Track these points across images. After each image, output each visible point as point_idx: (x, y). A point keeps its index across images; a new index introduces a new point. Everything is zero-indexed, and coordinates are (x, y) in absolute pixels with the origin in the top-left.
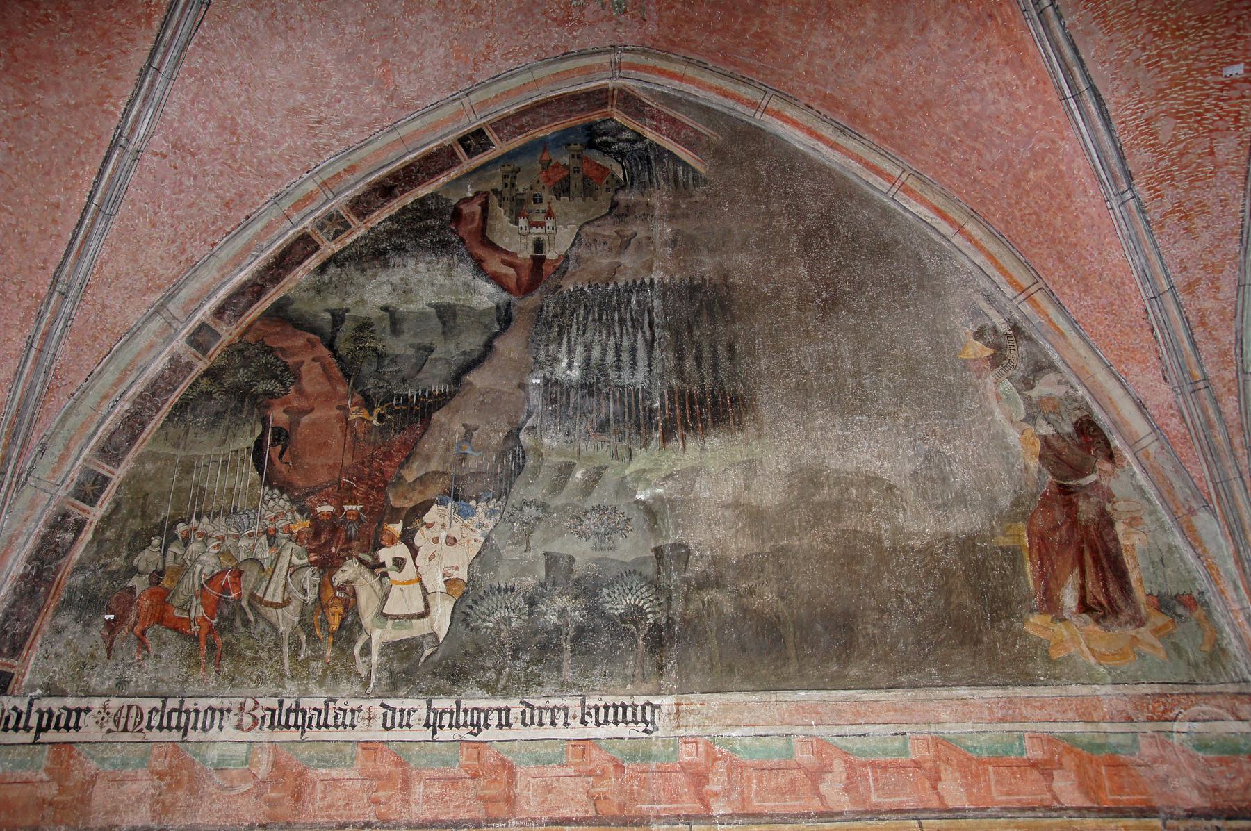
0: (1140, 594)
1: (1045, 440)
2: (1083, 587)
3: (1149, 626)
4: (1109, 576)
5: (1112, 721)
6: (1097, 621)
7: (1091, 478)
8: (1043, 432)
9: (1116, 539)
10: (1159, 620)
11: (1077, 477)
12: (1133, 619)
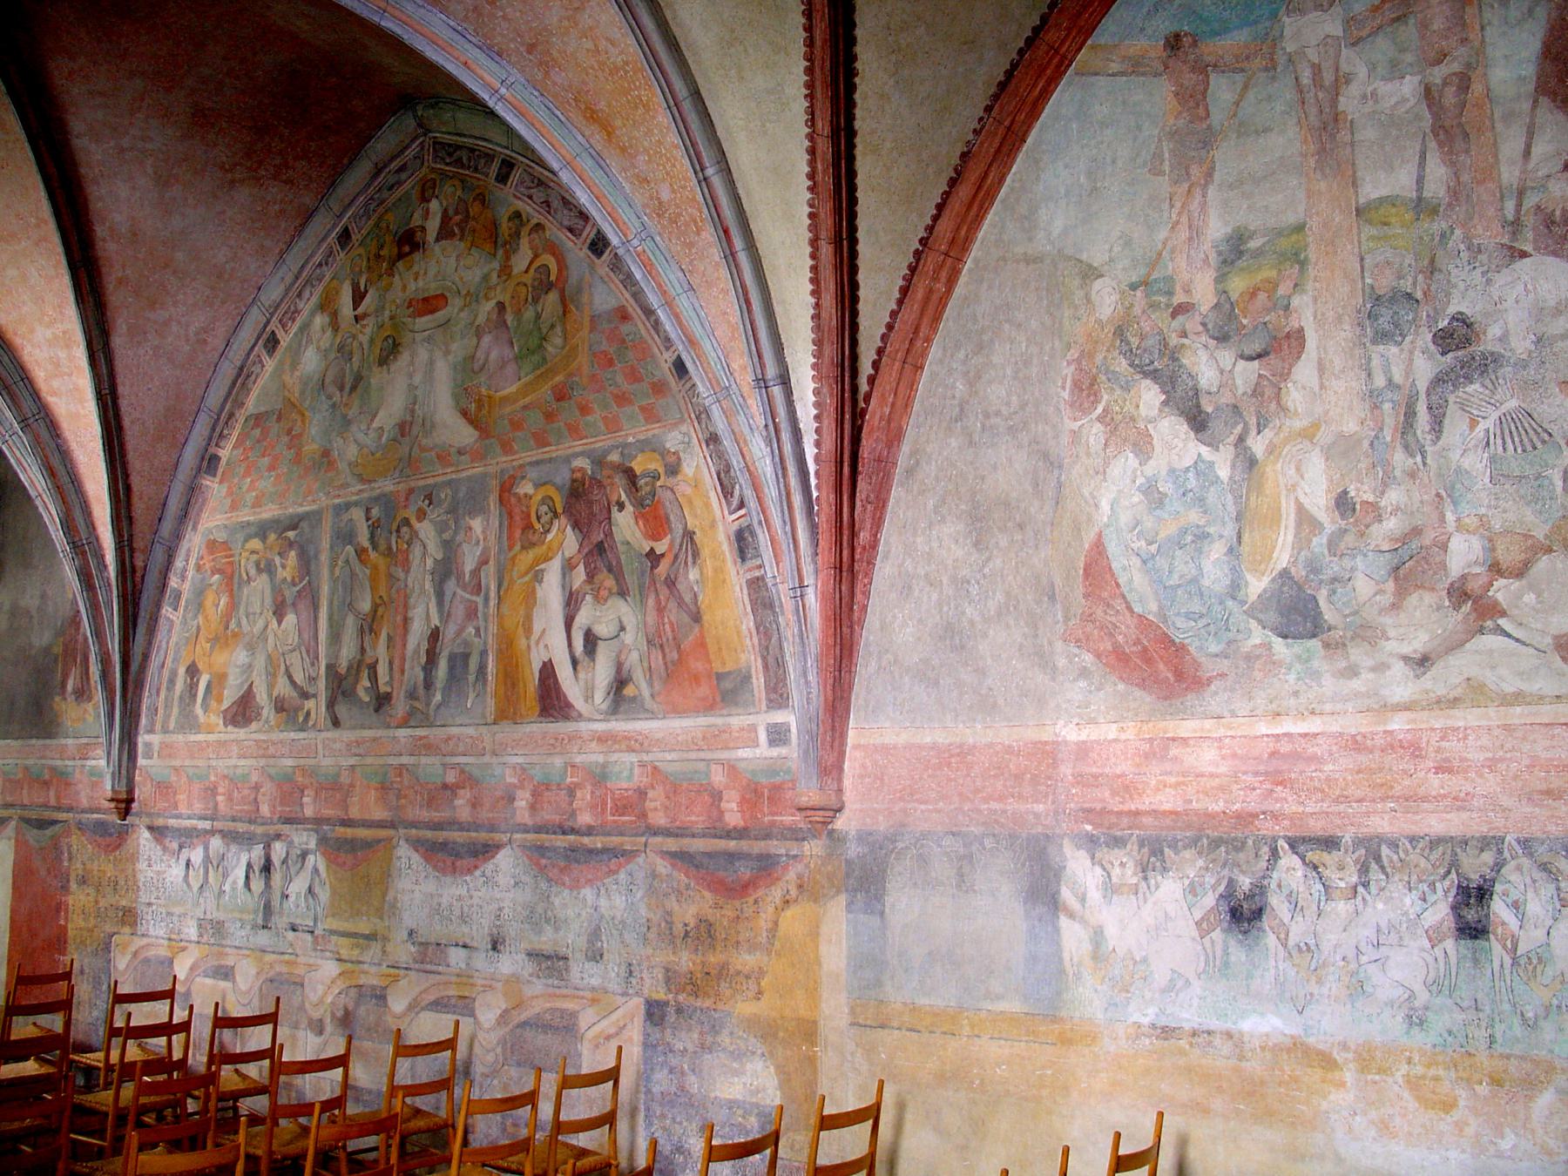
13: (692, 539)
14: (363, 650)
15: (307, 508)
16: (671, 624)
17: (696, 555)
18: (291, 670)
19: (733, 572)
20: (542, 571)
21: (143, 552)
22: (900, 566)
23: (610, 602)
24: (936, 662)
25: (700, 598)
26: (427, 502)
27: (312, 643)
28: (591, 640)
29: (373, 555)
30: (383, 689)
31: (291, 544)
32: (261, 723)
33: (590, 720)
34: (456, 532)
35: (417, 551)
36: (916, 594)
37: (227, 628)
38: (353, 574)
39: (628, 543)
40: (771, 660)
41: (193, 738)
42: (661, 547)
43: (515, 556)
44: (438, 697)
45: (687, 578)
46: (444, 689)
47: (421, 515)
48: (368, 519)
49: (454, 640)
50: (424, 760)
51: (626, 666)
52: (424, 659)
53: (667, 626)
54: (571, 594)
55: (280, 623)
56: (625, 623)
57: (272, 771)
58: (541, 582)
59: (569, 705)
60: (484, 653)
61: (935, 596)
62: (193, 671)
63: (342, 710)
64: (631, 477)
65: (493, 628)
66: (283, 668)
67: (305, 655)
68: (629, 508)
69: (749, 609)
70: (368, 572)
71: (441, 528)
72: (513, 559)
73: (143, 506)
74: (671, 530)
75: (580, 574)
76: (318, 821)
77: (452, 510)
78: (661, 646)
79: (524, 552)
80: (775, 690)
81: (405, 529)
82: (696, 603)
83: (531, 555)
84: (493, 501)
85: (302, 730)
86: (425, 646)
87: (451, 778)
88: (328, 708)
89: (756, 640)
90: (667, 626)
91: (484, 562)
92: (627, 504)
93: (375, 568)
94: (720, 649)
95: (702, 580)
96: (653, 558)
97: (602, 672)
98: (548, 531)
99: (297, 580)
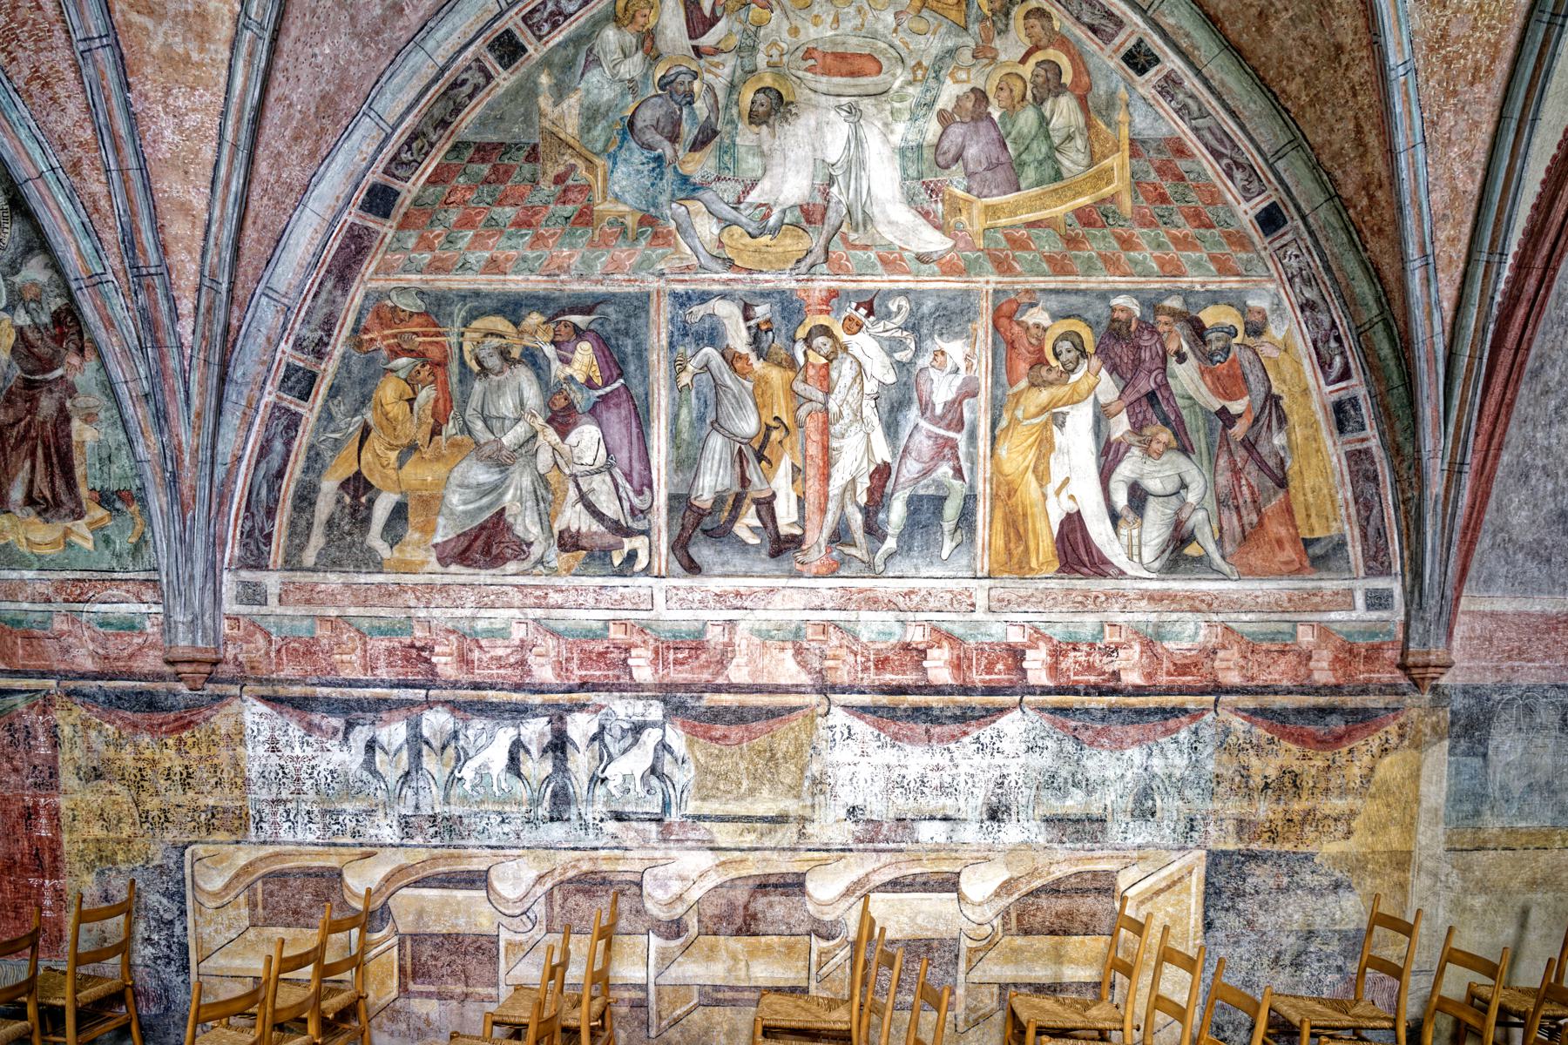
0: (83, 491)
1: (20, 331)
2: (31, 482)
3: (87, 519)
4: (57, 471)
5: (33, 602)
6: (39, 514)
7: (58, 372)
8: (19, 322)
9: (69, 436)
10: (99, 513)
11: (45, 371)
12: (73, 511)
13: (1278, 406)
14: (744, 481)
15: (611, 289)
16: (1249, 485)
17: (1282, 420)
18: (592, 498)
19: (1329, 443)
20: (1064, 414)
21: (240, 306)
22: (1520, 456)
23: (1164, 458)
24: (1549, 543)
25: (1288, 465)
26: (863, 311)
27: (637, 466)
28: (1138, 496)
29: (758, 365)
30: (784, 530)
31: (579, 333)
32: (526, 565)
33: (1136, 578)
34: (916, 353)
35: (844, 372)
36: (1533, 482)
37: (436, 431)
38: (717, 386)
39: (1190, 398)
40: (1371, 531)
41: (363, 579)
42: (1236, 407)
43: (1021, 392)
44: (891, 543)
45: (1270, 441)
46: (900, 536)
47: (853, 326)
48: (747, 319)
49: (916, 481)
50: (865, 615)
51: (1190, 524)
52: (863, 499)
53: (1244, 488)
54: (1108, 444)
55: (563, 434)
56: (1188, 480)
57: (561, 627)
58: (1062, 426)
59: (1106, 562)
60: (970, 499)
61: (1550, 487)
62: (358, 486)
63: (703, 552)
64: (1198, 331)
65: (984, 469)
66: (573, 494)
67: (621, 480)
68: (1192, 361)
69: (1347, 478)
70: (749, 385)
71: (892, 346)
72: (1018, 395)
73: (255, 236)
74: (1249, 391)
75: (1120, 426)
76: (665, 692)
77: (913, 327)
78: (1237, 508)
79: (1034, 390)
80: (1375, 558)
81: (819, 341)
82: (1283, 469)
83: (1044, 396)
84: (984, 324)
85: (620, 573)
86: (864, 483)
87: (916, 636)
88: (672, 548)
89: (1353, 510)
90: (1244, 488)
91: (969, 391)
92: (1190, 355)
93: (761, 382)
94: (1308, 516)
95: (1290, 447)
96: (1224, 415)
97: (1154, 530)
98: (1072, 371)
99: (598, 381)
